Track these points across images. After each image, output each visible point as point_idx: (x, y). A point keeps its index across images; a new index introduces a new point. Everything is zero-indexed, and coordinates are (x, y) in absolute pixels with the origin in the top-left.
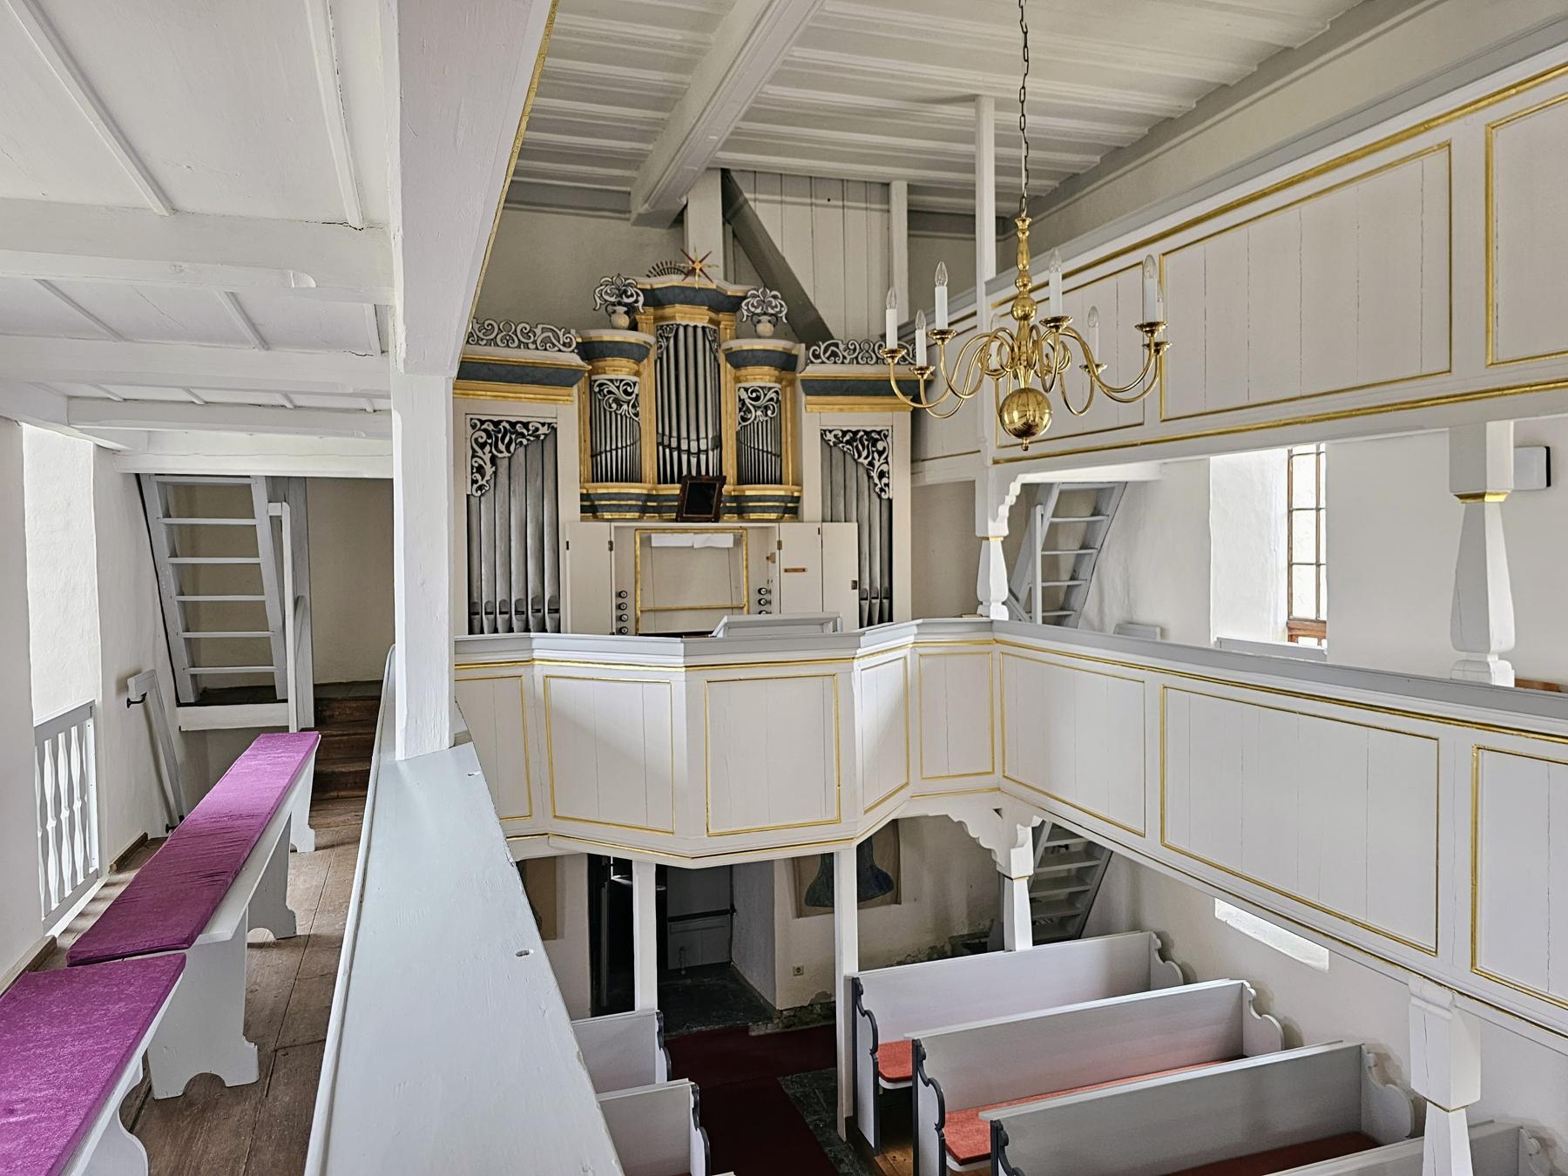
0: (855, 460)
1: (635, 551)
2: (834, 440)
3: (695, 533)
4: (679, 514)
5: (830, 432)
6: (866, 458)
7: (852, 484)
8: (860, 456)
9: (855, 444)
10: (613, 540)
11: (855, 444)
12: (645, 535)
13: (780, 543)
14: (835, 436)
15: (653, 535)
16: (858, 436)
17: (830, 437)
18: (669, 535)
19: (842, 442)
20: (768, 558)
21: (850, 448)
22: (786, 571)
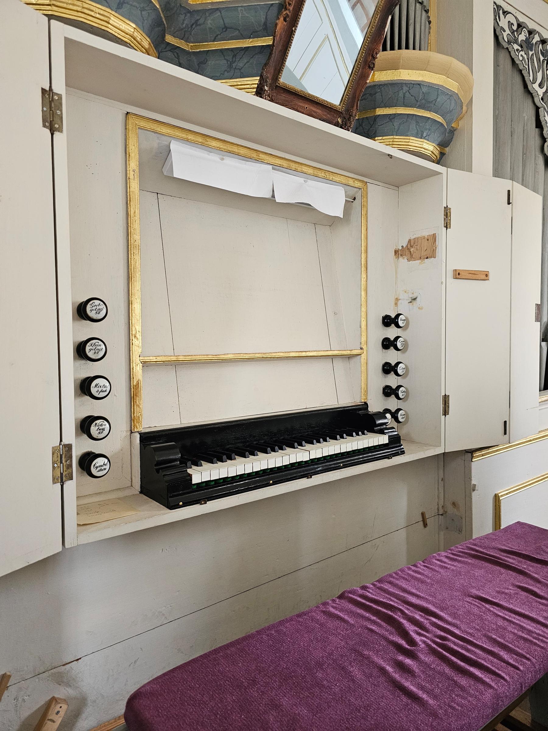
0: (525, 86)
1: (127, 179)
2: (508, 32)
3: (276, 167)
4: (269, 76)
5: (505, 13)
6: (541, 86)
7: (519, 130)
8: (534, 82)
9: (531, 53)
10: (59, 87)
11: (531, 53)
12: (154, 142)
13: (447, 212)
14: (510, 24)
15: (175, 146)
16: (534, 41)
17: (503, 22)
18: (214, 157)
19: (516, 41)
20: (396, 252)
21: (525, 56)
22: (457, 275)
